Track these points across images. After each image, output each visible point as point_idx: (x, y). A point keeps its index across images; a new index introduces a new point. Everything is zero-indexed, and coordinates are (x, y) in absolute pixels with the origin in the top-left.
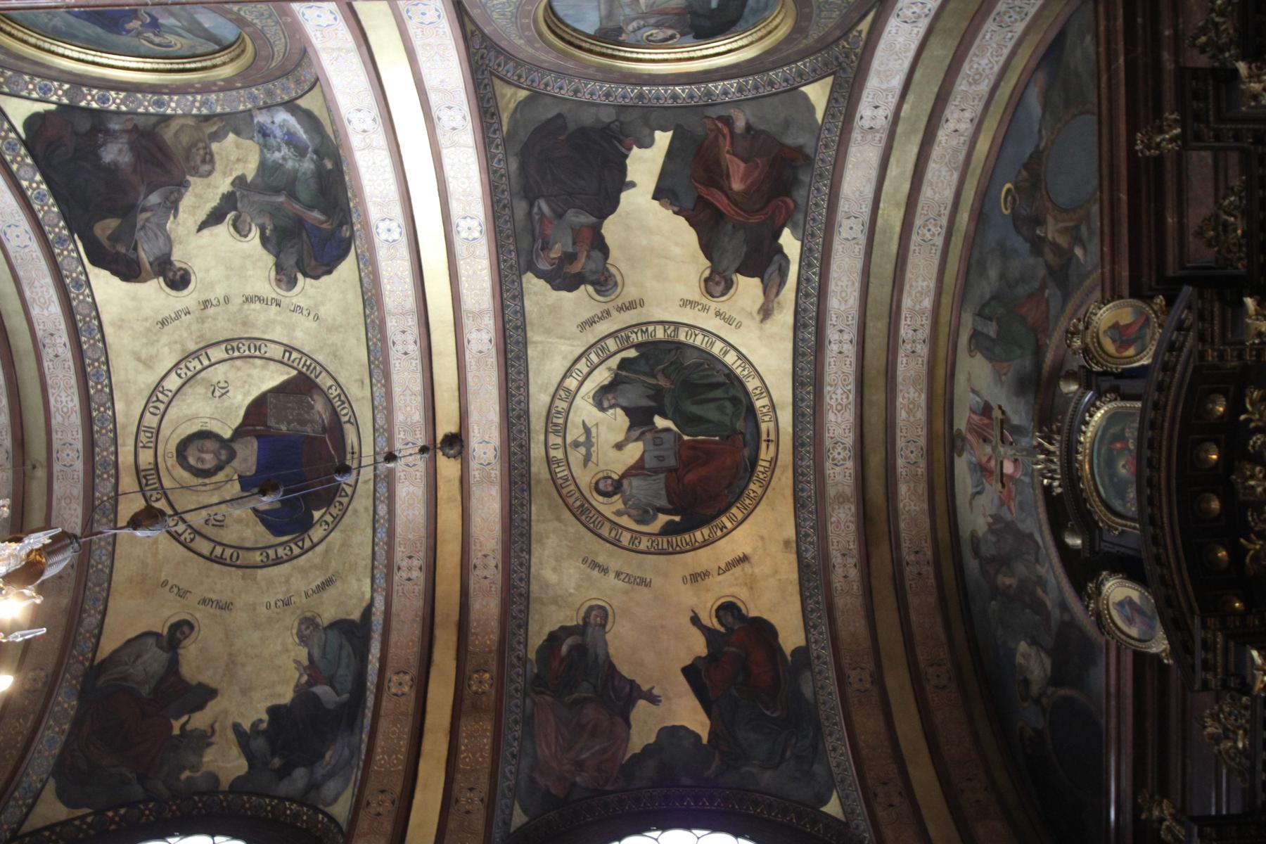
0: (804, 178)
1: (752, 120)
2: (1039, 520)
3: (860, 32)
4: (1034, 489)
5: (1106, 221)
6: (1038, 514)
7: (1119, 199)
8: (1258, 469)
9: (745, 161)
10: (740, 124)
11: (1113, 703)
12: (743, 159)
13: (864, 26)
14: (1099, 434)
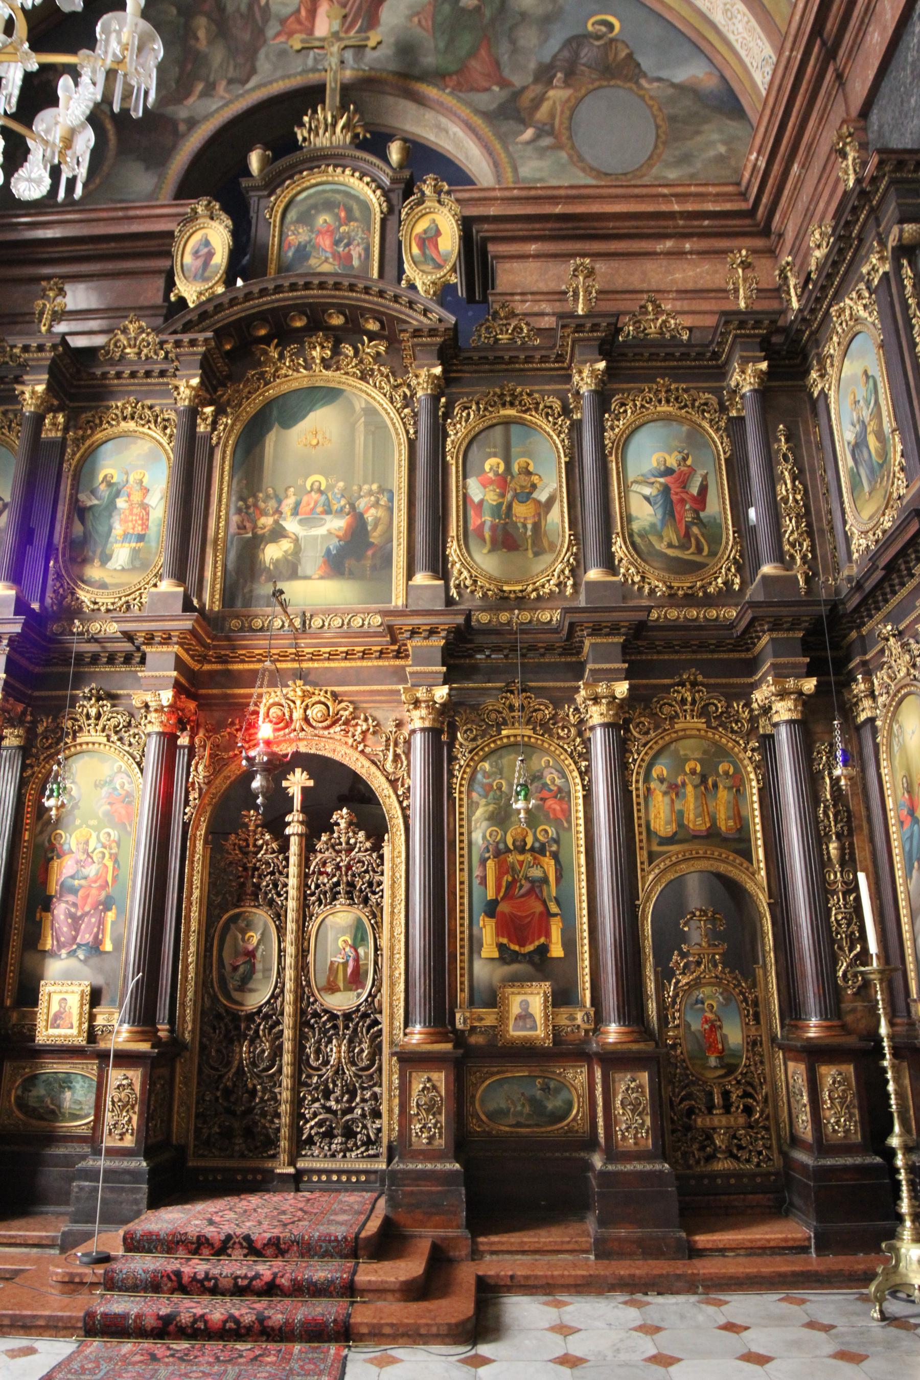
2: (271, 83)
4: (300, 74)
5: (540, 192)
6: (276, 81)
7: (558, 204)
8: (329, 353)
14: (353, 192)
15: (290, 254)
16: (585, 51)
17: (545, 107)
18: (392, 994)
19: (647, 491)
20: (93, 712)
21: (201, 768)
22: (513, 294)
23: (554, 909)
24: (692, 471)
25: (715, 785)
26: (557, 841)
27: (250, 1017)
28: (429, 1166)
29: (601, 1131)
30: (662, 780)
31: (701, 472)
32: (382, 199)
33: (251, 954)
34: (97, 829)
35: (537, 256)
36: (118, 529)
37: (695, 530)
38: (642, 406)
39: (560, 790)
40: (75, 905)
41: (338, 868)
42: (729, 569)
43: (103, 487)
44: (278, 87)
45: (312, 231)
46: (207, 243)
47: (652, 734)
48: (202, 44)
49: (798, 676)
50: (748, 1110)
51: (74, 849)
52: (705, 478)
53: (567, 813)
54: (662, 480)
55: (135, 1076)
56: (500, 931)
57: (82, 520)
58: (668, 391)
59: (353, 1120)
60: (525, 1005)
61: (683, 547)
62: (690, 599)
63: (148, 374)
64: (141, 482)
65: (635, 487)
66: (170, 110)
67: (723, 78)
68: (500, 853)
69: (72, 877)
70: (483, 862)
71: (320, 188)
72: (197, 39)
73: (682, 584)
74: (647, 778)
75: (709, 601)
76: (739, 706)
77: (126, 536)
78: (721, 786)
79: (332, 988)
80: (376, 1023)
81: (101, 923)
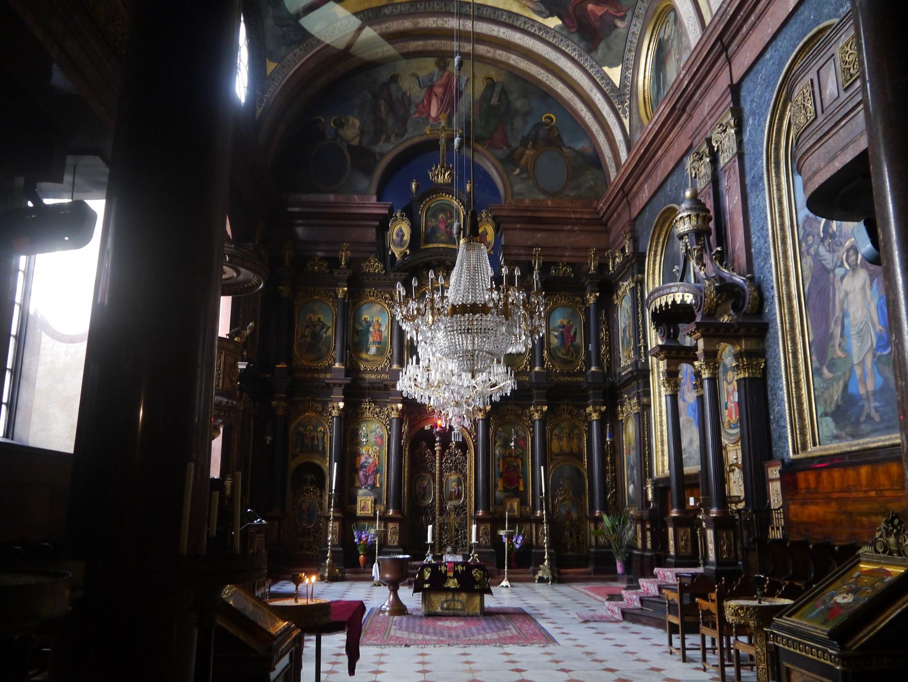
0: (583, 44)
1: (619, 31)
3: (626, 118)
9: (601, 16)
10: (619, 23)
11: (361, 205)
12: (604, 14)
13: (626, 122)
15: (429, 230)
16: (541, 131)
17: (525, 158)
18: (470, 501)
19: (556, 334)
20: (368, 407)
21: (406, 427)
22: (510, 246)
23: (521, 475)
24: (572, 327)
25: (573, 437)
26: (522, 454)
27: (426, 508)
28: (486, 550)
29: (534, 540)
30: (556, 435)
31: (575, 327)
32: (464, 210)
33: (425, 488)
34: (372, 447)
35: (520, 229)
36: (371, 339)
37: (571, 349)
38: (556, 301)
39: (523, 437)
40: (366, 472)
41: (452, 461)
42: (582, 364)
43: (364, 322)
44: (417, 140)
45: (437, 221)
46: (401, 231)
47: (554, 420)
48: (384, 115)
49: (600, 406)
50: (578, 538)
51: (364, 453)
52: (576, 329)
53: (526, 445)
54: (561, 330)
55: (397, 525)
56: (504, 482)
57: (358, 335)
58: (565, 296)
59: (458, 540)
60: (512, 505)
61: (567, 354)
62: (569, 374)
63: (379, 280)
64: (378, 321)
65: (552, 332)
66: (372, 147)
67: (594, 148)
68: (504, 457)
69: (365, 463)
70: (499, 460)
71: (440, 202)
72: (380, 111)
73: (566, 368)
74: (551, 435)
75: (576, 375)
76: (582, 411)
77: (374, 342)
78: (575, 438)
79: (451, 499)
80: (465, 510)
81: (375, 478)
